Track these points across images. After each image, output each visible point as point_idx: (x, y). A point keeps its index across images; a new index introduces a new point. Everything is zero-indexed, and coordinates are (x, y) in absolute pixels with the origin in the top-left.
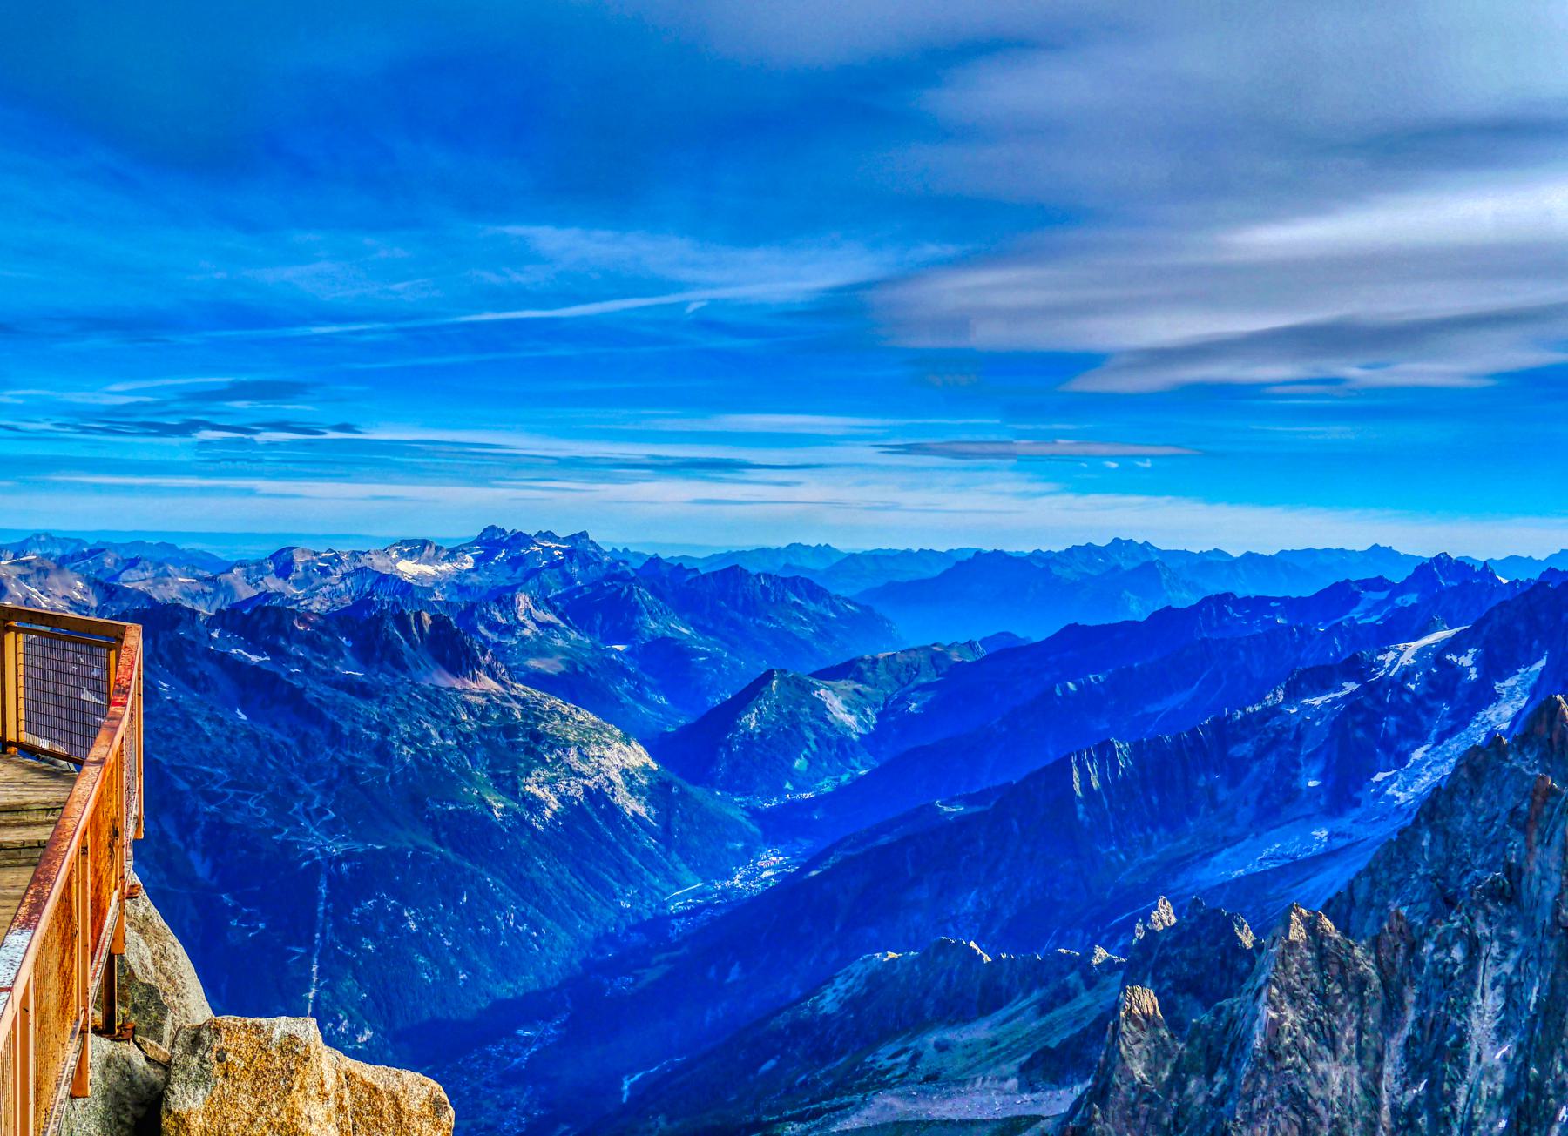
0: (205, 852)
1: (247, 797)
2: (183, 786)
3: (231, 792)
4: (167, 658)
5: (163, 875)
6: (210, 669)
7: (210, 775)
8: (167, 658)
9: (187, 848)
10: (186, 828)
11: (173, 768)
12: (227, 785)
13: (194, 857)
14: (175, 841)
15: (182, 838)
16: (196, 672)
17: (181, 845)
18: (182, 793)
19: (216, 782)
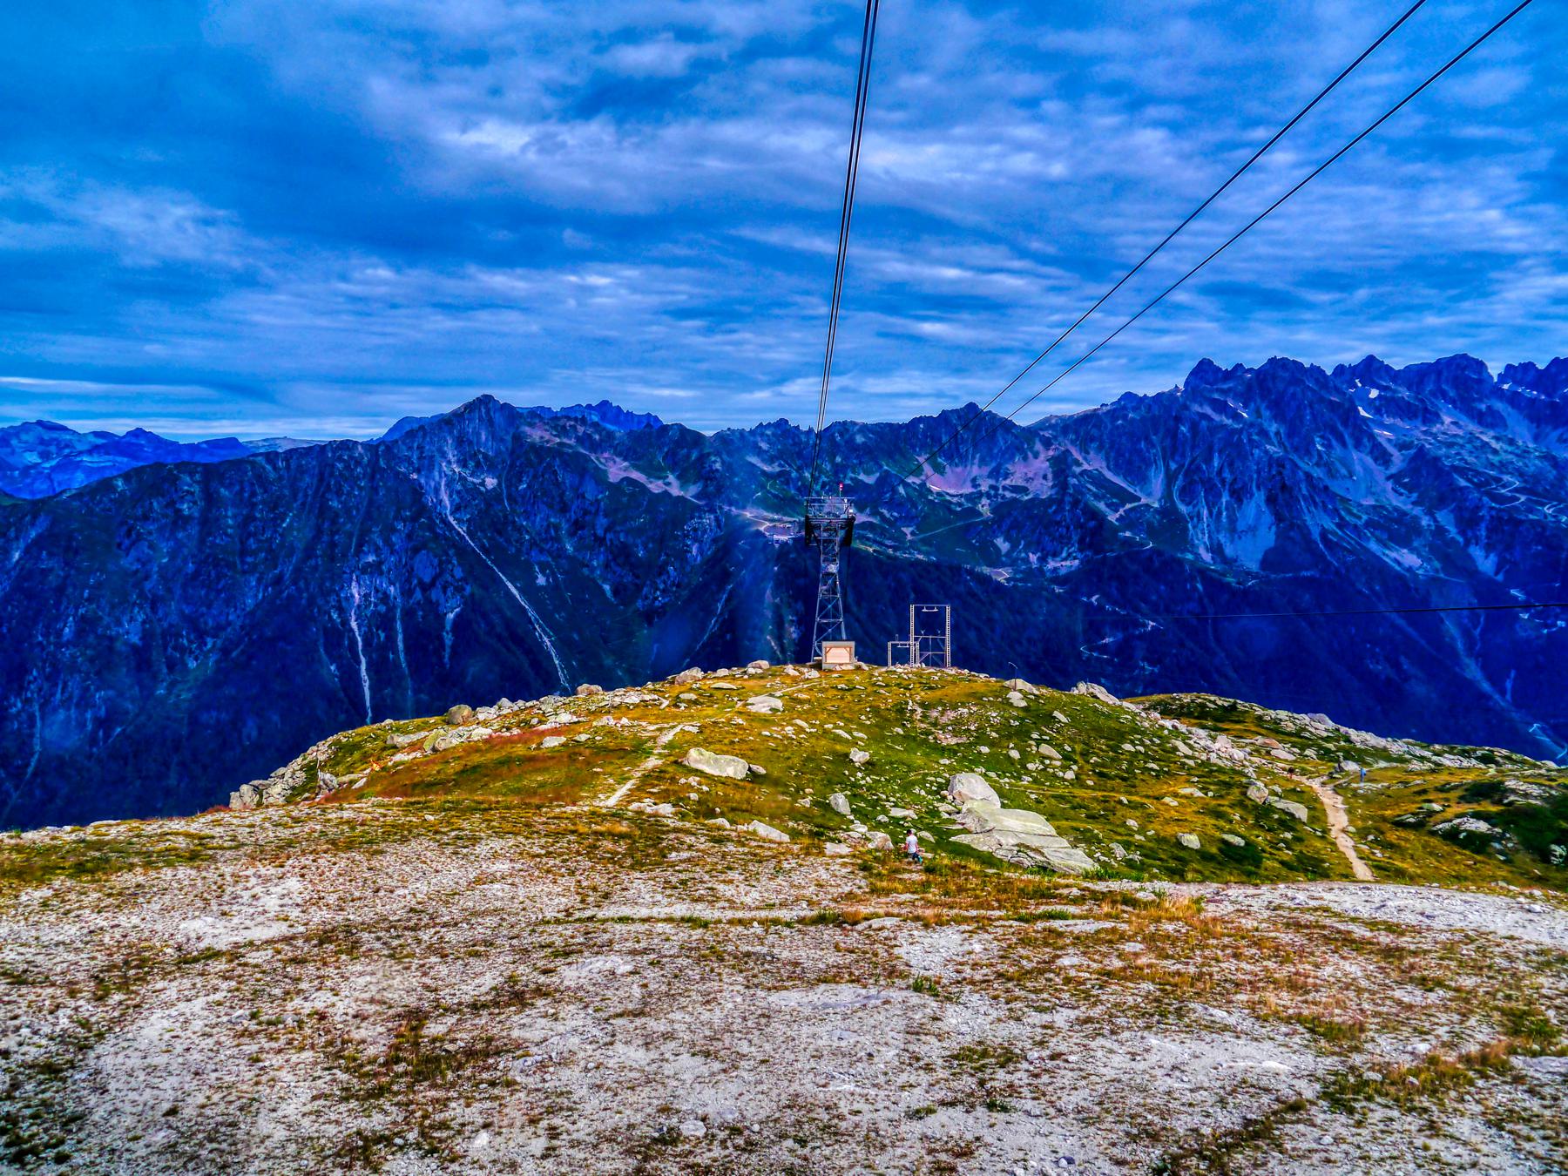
0: (1489, 548)
1: (1543, 505)
2: (1463, 483)
3: (1523, 498)
4: (1452, 394)
5: (1437, 564)
6: (1499, 406)
7: (1498, 480)
8: (1452, 394)
9: (1467, 543)
10: (1468, 522)
11: (1455, 468)
12: (1517, 490)
13: (1477, 552)
14: (1453, 531)
15: (1462, 533)
16: (1483, 407)
17: (1460, 539)
18: (1462, 489)
19: (1504, 486)
